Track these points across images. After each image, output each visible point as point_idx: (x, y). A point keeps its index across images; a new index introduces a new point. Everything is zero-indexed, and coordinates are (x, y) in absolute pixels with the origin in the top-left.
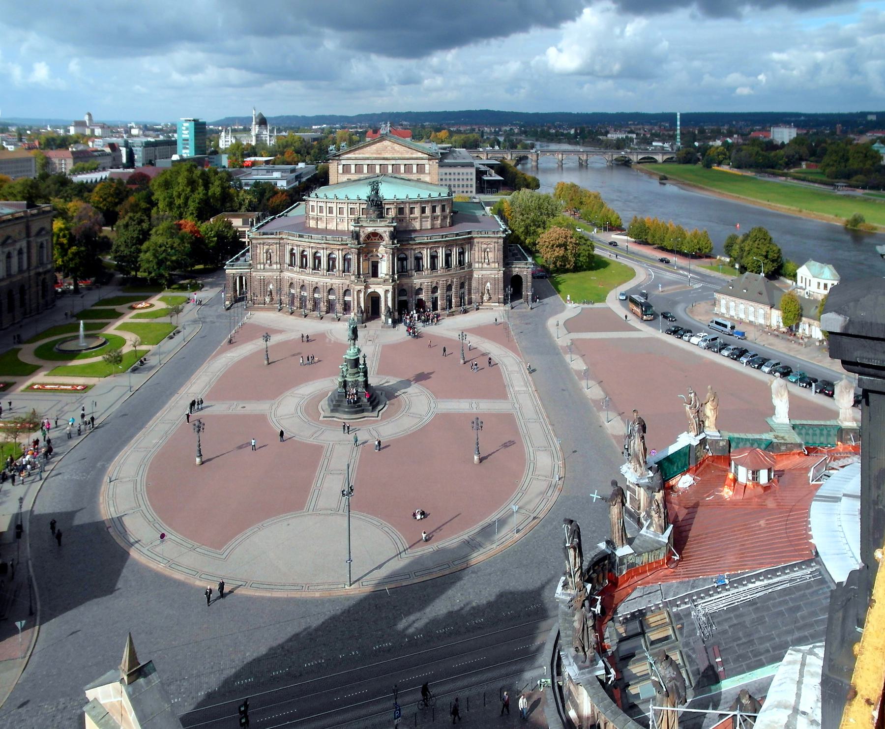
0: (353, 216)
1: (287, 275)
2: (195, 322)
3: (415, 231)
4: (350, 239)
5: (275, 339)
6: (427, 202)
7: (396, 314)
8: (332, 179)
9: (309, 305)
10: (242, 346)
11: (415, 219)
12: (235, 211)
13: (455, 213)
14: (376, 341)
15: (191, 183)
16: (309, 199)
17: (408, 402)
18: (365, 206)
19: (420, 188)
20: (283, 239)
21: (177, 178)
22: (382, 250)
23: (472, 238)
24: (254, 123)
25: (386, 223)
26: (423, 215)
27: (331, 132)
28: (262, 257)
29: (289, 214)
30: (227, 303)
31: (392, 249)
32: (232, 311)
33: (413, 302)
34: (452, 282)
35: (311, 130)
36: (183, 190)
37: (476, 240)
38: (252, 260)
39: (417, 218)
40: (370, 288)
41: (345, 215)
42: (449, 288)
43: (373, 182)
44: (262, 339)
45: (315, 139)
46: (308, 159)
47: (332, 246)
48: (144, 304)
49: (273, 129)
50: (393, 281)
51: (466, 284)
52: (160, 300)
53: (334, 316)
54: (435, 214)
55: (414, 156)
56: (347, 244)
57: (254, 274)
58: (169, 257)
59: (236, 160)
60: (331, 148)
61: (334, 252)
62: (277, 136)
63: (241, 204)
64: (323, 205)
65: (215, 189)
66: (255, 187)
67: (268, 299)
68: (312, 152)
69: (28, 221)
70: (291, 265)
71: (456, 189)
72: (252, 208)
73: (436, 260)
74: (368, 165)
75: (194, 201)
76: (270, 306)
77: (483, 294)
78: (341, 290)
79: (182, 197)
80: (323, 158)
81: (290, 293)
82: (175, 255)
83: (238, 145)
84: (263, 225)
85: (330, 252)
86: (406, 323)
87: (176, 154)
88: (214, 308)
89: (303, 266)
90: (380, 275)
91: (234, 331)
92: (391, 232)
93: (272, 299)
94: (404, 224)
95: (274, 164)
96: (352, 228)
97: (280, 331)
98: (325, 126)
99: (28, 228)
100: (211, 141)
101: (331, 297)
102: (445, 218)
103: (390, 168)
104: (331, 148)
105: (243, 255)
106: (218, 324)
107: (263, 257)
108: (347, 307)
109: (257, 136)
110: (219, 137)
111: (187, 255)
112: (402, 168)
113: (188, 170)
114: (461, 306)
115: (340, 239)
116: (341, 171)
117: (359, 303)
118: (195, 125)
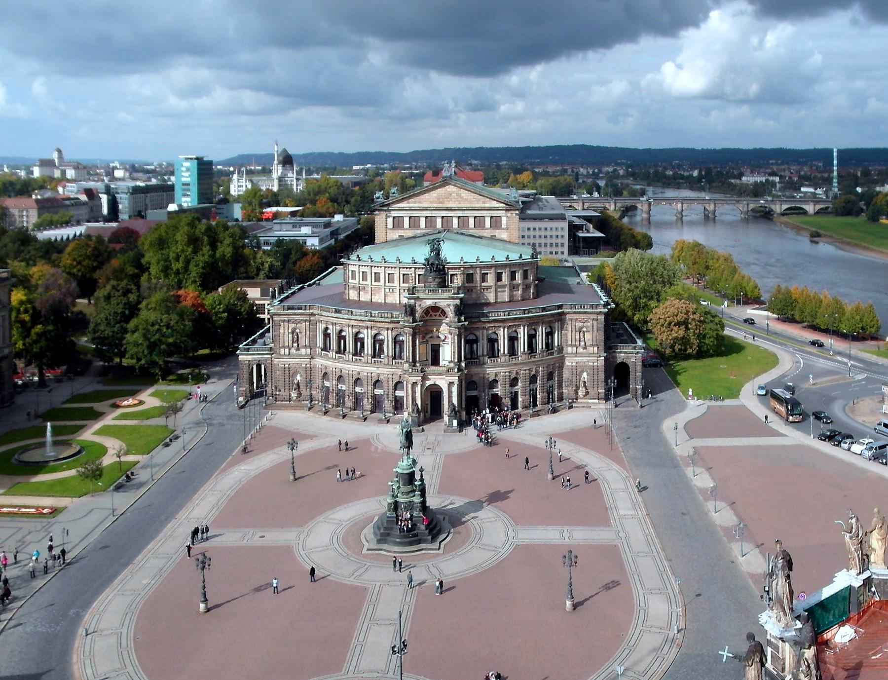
0: (407, 285)
1: (319, 362)
2: (198, 424)
3: (488, 304)
4: (403, 315)
5: (303, 447)
6: (504, 266)
7: (464, 413)
9: (349, 403)
10: (260, 456)
11: (488, 288)
12: (251, 278)
13: (541, 280)
14: (437, 449)
15: (194, 241)
16: (349, 262)
17: (479, 530)
18: (422, 272)
19: (495, 247)
21: (174, 235)
22: (444, 329)
23: (563, 314)
24: (276, 162)
25: (450, 294)
26: (499, 283)
27: (378, 174)
28: (286, 339)
29: (322, 282)
30: (241, 399)
31: (458, 328)
32: (247, 409)
33: (485, 398)
34: (537, 371)
35: (351, 171)
36: (183, 251)
37: (568, 317)
38: (273, 342)
39: (490, 287)
40: (429, 379)
41: (396, 283)
42: (533, 379)
43: (433, 240)
44: (286, 447)
45: (356, 184)
46: (347, 209)
47: (379, 325)
48: (131, 401)
49: (301, 170)
50: (459, 370)
51: (556, 374)
52: (152, 395)
53: (381, 416)
54: (514, 282)
55: (487, 205)
57: (276, 361)
58: (164, 339)
59: (253, 211)
60: (377, 195)
61: (382, 332)
62: (306, 179)
63: (258, 269)
64: (367, 270)
65: (225, 249)
66: (278, 247)
67: (294, 395)
68: (353, 200)
70: (325, 349)
71: (543, 249)
72: (274, 274)
73: (516, 342)
74: (426, 217)
75: (197, 266)
76: (297, 403)
77: (578, 388)
78: (390, 382)
79: (181, 259)
80: (367, 208)
81: (323, 386)
82: (172, 336)
83: (255, 192)
84: (287, 297)
85: (376, 332)
86: (476, 426)
87: (174, 203)
88: (223, 406)
89: (341, 351)
90: (442, 363)
91: (249, 437)
92: (456, 306)
93: (300, 395)
94: (474, 296)
95: (302, 216)
96: (405, 301)
97: (311, 437)
98: (369, 165)
100: (219, 186)
101: (378, 392)
102: (527, 287)
103: (455, 221)
104: (377, 195)
105: (262, 336)
106: (228, 427)
107: (287, 339)
108: (398, 405)
109: (280, 179)
110: (230, 181)
111: (188, 336)
113: (189, 224)
114: (548, 403)
115: (390, 316)
116: (390, 226)
117: (414, 399)
118: (199, 164)
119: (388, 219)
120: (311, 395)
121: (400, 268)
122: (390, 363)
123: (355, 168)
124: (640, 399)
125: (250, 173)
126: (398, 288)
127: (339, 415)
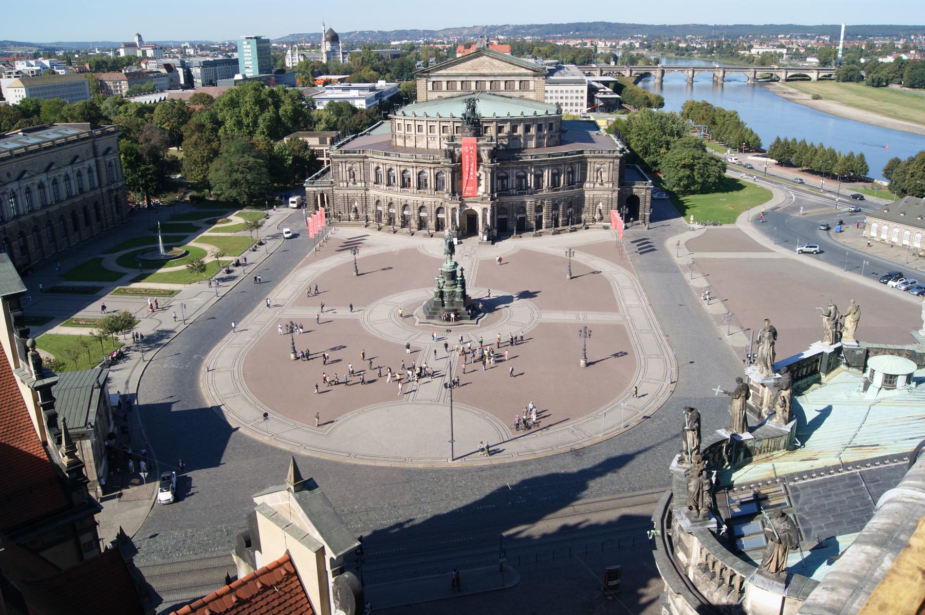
0: (445, 135)
8: (421, 95)
9: (398, 222)
16: (395, 117)
18: (459, 125)
19: (523, 105)
20: (367, 158)
28: (344, 175)
29: (371, 133)
41: (437, 133)
43: (469, 99)
50: (492, 199)
56: (439, 163)
60: (418, 64)
61: (425, 171)
64: (412, 123)
65: (286, 108)
67: (352, 216)
69: (94, 141)
70: (376, 183)
72: (331, 127)
73: (541, 179)
76: (356, 222)
78: (433, 208)
79: (251, 115)
81: (377, 211)
84: (343, 144)
85: (420, 170)
87: (238, 73)
93: (357, 217)
96: (445, 147)
99: (94, 148)
103: (488, 85)
104: (418, 64)
105: (324, 173)
107: (345, 175)
108: (440, 226)
112: (502, 85)
114: (568, 225)
115: (432, 158)
119: (428, 83)
120: (367, 216)
121: (440, 122)
122: (433, 193)
123: (393, 43)
124: (647, 222)
125: (301, 48)
126: (438, 137)
127: (390, 231)
